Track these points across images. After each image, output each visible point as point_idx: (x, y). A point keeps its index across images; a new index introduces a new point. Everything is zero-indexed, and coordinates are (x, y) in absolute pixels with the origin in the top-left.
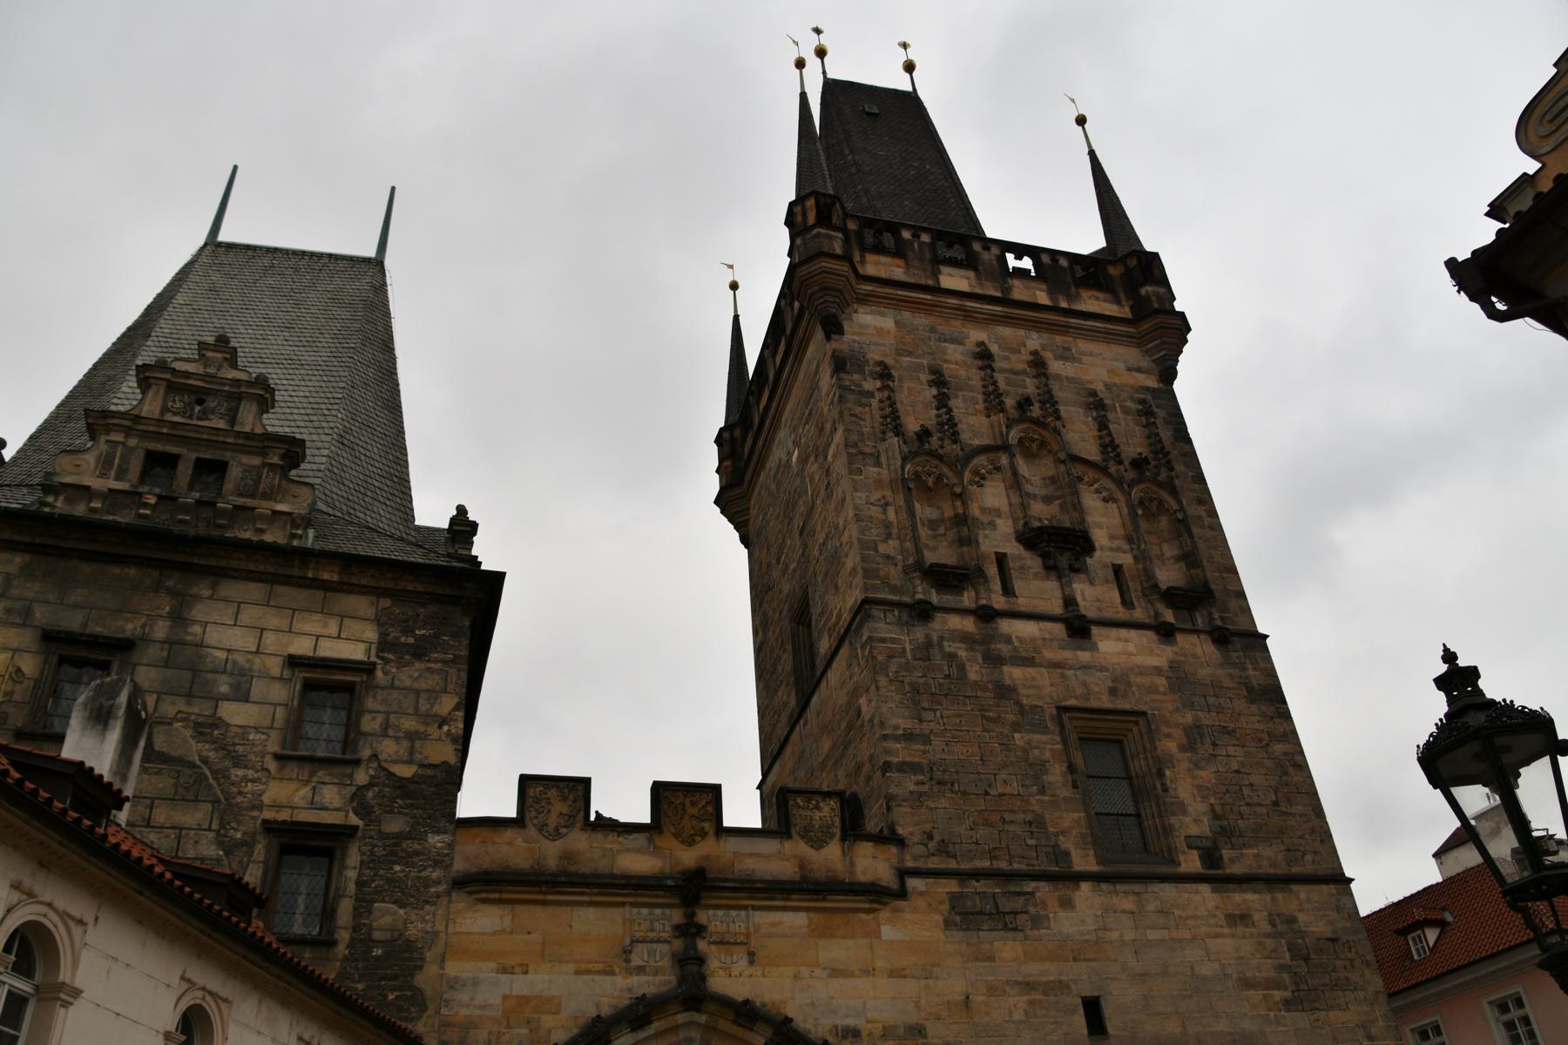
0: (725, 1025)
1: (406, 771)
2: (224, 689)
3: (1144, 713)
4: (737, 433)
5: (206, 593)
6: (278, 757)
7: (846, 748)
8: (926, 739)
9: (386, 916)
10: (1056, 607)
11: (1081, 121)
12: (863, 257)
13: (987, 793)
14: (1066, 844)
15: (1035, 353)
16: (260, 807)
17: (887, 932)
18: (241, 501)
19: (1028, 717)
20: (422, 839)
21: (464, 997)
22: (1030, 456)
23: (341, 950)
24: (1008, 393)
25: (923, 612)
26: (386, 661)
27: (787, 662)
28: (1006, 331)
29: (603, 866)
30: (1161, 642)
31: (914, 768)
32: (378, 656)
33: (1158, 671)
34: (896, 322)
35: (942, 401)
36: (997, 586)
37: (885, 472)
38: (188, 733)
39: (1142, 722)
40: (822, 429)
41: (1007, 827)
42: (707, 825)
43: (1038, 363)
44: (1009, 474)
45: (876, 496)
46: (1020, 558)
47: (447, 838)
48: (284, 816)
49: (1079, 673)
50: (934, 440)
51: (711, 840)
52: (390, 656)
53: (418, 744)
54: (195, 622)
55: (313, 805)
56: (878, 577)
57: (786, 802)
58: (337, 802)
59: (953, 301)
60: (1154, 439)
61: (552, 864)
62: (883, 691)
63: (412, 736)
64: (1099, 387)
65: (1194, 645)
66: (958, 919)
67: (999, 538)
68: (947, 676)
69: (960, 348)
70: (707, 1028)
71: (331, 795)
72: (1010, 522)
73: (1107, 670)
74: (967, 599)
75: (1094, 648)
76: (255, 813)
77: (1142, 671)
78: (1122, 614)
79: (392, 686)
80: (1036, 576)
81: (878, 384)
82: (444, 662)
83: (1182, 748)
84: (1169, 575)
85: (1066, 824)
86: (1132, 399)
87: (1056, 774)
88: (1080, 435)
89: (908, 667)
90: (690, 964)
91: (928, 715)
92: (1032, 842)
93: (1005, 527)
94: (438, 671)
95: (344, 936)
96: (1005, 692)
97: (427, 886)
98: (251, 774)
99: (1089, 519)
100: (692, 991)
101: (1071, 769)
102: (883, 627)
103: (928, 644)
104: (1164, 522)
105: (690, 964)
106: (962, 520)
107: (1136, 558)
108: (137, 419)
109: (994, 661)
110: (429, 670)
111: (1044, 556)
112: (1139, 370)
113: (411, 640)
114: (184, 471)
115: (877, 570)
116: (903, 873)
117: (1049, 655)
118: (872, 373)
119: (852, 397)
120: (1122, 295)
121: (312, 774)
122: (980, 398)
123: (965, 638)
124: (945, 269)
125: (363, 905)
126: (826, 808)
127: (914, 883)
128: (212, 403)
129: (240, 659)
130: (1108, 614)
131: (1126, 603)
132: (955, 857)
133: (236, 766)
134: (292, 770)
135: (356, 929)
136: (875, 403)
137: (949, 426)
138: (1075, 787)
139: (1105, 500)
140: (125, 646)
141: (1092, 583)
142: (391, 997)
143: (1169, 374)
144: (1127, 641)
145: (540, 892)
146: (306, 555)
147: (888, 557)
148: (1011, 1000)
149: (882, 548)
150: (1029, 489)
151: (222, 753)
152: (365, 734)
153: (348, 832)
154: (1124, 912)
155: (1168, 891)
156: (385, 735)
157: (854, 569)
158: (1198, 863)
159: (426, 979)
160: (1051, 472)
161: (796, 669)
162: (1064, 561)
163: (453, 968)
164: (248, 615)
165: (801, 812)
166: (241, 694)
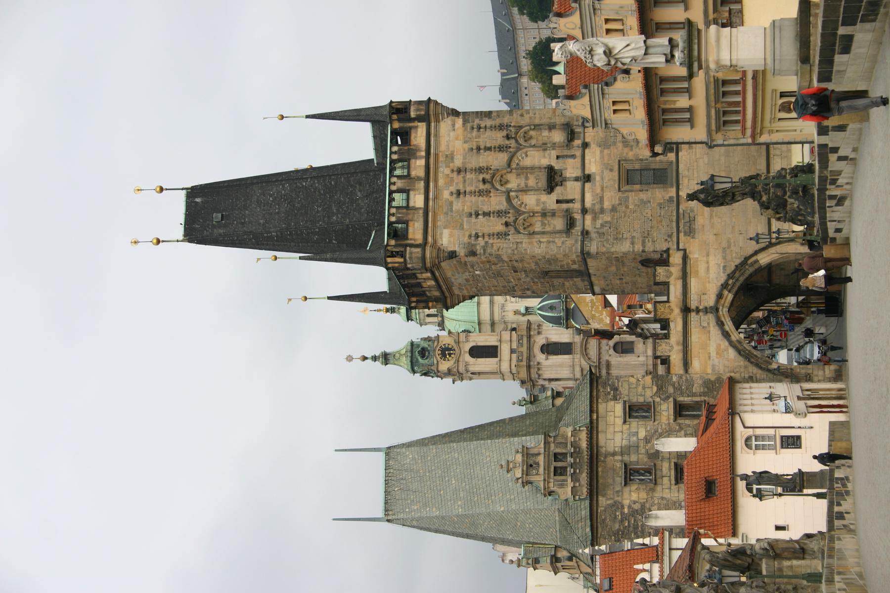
0: (722, 301)
1: (655, 389)
2: (635, 438)
3: (619, 161)
4: (414, 299)
8: (633, 237)
10: (578, 185)
11: (282, 117)
14: (667, 197)
15: (453, 171)
16: (669, 424)
17: (696, 256)
18: (569, 445)
19: (624, 202)
21: (717, 368)
22: (507, 182)
23: (706, 398)
24: (476, 187)
25: (585, 233)
27: (556, 282)
28: (441, 182)
29: (681, 334)
33: (602, 152)
35: (486, 214)
36: (570, 205)
40: (489, 262)
43: (459, 171)
45: (536, 244)
48: (672, 417)
50: (507, 219)
59: (431, 203)
60: (492, 128)
61: (681, 347)
63: (644, 388)
64: (466, 146)
67: (549, 201)
71: (664, 407)
73: (602, 172)
74: (578, 216)
75: (594, 173)
77: (602, 157)
80: (565, 190)
83: (632, 150)
84: (558, 136)
85: (660, 196)
86: (471, 133)
87: (643, 196)
88: (498, 160)
89: (607, 240)
90: (706, 311)
91: (625, 236)
93: (544, 198)
95: (703, 398)
96: (614, 209)
99: (537, 164)
100: (715, 310)
102: (593, 248)
103: (598, 232)
104: (532, 133)
105: (706, 311)
106: (544, 215)
107: (553, 149)
108: (545, 480)
109: (602, 211)
112: (453, 125)
114: (559, 464)
116: (678, 249)
117: (598, 190)
119: (489, 251)
120: (411, 124)
122: (481, 198)
123: (594, 219)
124: (411, 204)
125: (694, 395)
127: (681, 247)
128: (531, 462)
130: (579, 165)
131: (573, 156)
134: (657, 417)
136: (491, 241)
137: (499, 213)
140: (626, 465)
141: (566, 169)
143: (455, 113)
146: (591, 422)
147: (563, 243)
150: (523, 185)
153: (675, 400)
155: (681, 166)
159: (713, 378)
161: (566, 278)
162: (558, 179)
163: (709, 371)
164: (609, 436)
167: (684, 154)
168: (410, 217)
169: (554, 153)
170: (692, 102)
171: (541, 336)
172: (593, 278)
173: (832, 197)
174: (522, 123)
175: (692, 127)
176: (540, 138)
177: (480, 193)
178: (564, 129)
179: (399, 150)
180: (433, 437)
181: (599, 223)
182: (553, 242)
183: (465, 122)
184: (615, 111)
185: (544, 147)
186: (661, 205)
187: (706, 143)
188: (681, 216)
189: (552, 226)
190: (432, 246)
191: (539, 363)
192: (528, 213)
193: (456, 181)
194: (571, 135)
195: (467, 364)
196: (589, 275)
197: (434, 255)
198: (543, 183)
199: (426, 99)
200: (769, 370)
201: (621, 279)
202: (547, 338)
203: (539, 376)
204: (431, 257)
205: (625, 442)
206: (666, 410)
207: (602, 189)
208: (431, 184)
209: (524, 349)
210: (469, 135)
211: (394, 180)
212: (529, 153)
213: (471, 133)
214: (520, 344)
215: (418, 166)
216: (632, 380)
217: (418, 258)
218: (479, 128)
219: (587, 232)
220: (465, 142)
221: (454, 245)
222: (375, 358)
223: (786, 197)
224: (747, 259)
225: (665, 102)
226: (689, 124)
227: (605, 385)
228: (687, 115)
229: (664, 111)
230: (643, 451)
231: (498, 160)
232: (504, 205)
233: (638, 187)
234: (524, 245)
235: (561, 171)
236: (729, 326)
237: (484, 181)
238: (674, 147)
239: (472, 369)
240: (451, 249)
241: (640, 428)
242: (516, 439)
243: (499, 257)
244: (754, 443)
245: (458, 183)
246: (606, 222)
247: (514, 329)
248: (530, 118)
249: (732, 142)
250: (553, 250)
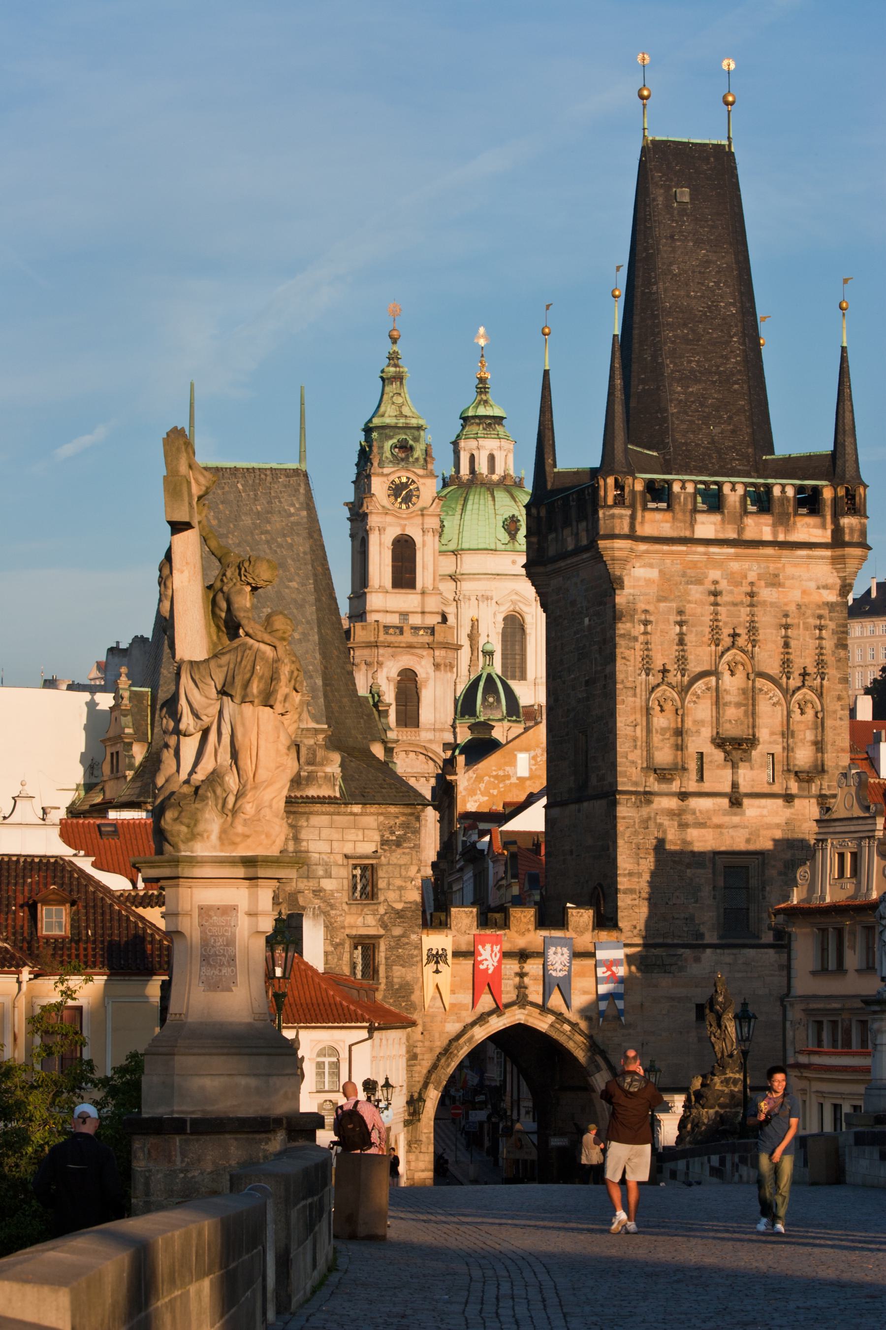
1: (399, 906)
4: (543, 513)
5: (305, 824)
10: (727, 789)
12: (643, 517)
14: (703, 929)
15: (752, 584)
16: (344, 928)
20: (408, 937)
23: (382, 987)
24: (726, 623)
25: (647, 796)
26: (385, 850)
28: (735, 566)
30: (785, 807)
31: (631, 891)
33: (778, 826)
34: (660, 571)
35: (681, 642)
36: (693, 775)
37: (638, 700)
38: (311, 895)
39: (760, 857)
43: (751, 595)
44: (714, 694)
45: (632, 718)
46: (711, 755)
48: (354, 932)
49: (730, 830)
51: (532, 932)
52: (386, 847)
54: (303, 840)
59: (701, 549)
63: (400, 888)
64: (792, 608)
65: (805, 808)
66: (643, 968)
67: (700, 741)
69: (700, 588)
70: (527, 1015)
72: (710, 729)
73: (747, 827)
74: (675, 787)
75: (743, 814)
76: (342, 930)
77: (769, 827)
78: (766, 789)
79: (389, 864)
80: (718, 767)
81: (642, 627)
82: (410, 848)
84: (803, 756)
86: (813, 615)
87: (706, 892)
89: (636, 833)
90: (521, 988)
91: (641, 860)
92: (685, 929)
93: (707, 733)
94: (408, 854)
95: (383, 980)
97: (412, 958)
98: (338, 912)
99: (760, 721)
100: (522, 1001)
101: (714, 887)
103: (649, 818)
104: (810, 713)
105: (521, 988)
106: (679, 732)
109: (683, 826)
110: (404, 853)
111: (725, 752)
112: (826, 587)
113: (394, 838)
117: (716, 820)
118: (641, 621)
121: (362, 910)
123: (671, 813)
124: (700, 517)
125: (389, 967)
129: (323, 856)
133: (332, 909)
134: (354, 908)
135: (387, 978)
136: (638, 646)
137: (682, 660)
138: (714, 898)
139: (774, 705)
141: (751, 769)
142: (403, 1004)
144: (764, 807)
147: (633, 762)
149: (630, 758)
150: (728, 698)
152: (381, 889)
153: (380, 937)
154: (726, 964)
155: (751, 952)
156: (389, 889)
158: (772, 939)
159: (415, 997)
160: (743, 686)
162: (737, 754)
164: (325, 833)
166: (329, 876)
167: (771, 954)
168: (680, 516)
169: (778, 749)
170: (852, 975)
171: (431, 669)
172: (573, 807)
173: (722, 1161)
174: (827, 699)
175: (814, 973)
176: (802, 727)
177: (715, 629)
178: (816, 766)
179: (788, 498)
180: (322, 547)
181: (666, 821)
182: (635, 747)
183: (831, 606)
184: (842, 856)
185: (788, 733)
186: (690, 919)
187: (788, 995)
188: (672, 951)
189: (660, 745)
190: (632, 550)
191: (380, 664)
192: (683, 707)
193: (736, 590)
194: (805, 777)
195: (381, 530)
196: (579, 801)
197: (617, 554)
198: (731, 730)
199: (869, 542)
200: (426, 1085)
201: (571, 852)
202: (427, 680)
204: (613, 549)
205: (315, 857)
206: (365, 922)
207: (719, 826)
208: (732, 550)
209: (408, 637)
210: (809, 612)
211: (740, 490)
212: (778, 708)
213: (813, 615)
214: (415, 629)
215: (760, 527)
216: (413, 870)
217: (613, 528)
218: (821, 628)
219: (649, 802)
220: (799, 606)
221: (634, 587)
222: (393, 358)
223: (717, 1108)
225: (853, 933)
226: (819, 968)
227: (406, 826)
228: (832, 965)
229: (840, 932)
230: (302, 885)
231: (768, 658)
232: (695, 668)
233: (721, 883)
234: (631, 699)
235: (749, 760)
236: (497, 1024)
237: (734, 635)
238: (782, 942)
239: (374, 540)
240: (626, 583)
241: (336, 883)
242: (319, 682)
243: (611, 658)
244: (327, 1060)
245: (731, 594)
247: (444, 619)
248: (835, 712)
249: (790, 1034)
250: (622, 747)
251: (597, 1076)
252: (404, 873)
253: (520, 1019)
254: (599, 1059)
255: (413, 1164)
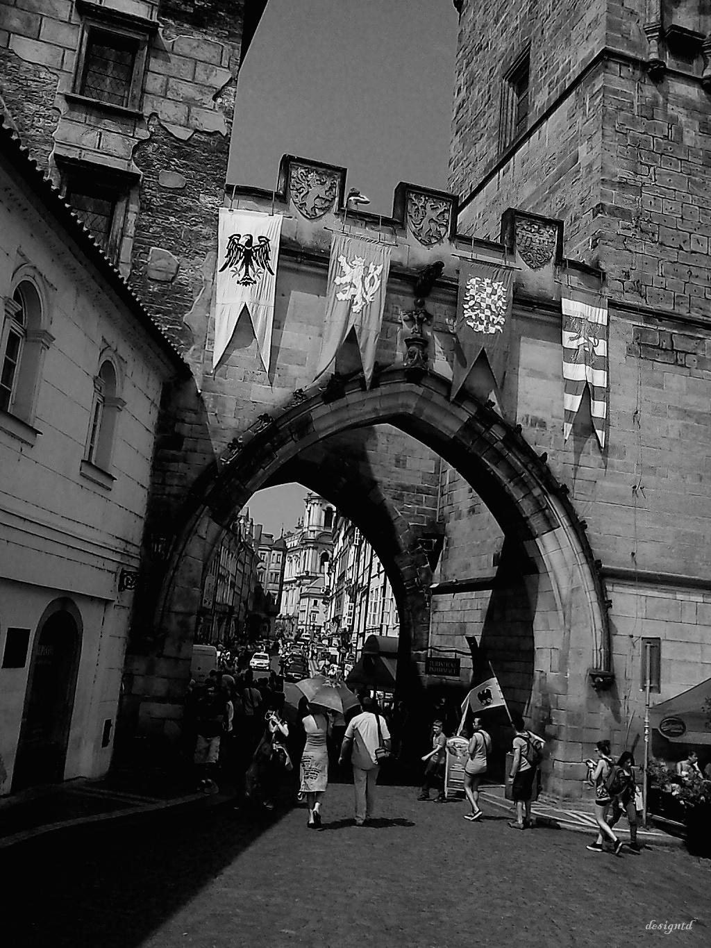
0: (438, 399)
1: (183, 134)
6: (68, 99)
7: (553, 192)
9: (160, 260)
13: (681, 248)
26: (167, 26)
31: (624, 214)
32: (158, 19)
41: (692, 280)
42: (443, 230)
47: (217, 200)
48: (73, 154)
53: (194, 109)
55: (98, 150)
56: (619, 31)
57: (513, 223)
58: (121, 151)
62: (607, 140)
63: (189, 102)
66: (637, 348)
68: (666, 137)
70: (423, 398)
76: (47, 148)
89: (633, 121)
97: (197, 239)
103: (655, 104)
115: (620, 24)
123: (688, 105)
125: (141, 247)
126: (546, 235)
132: (644, 297)
145: (296, 262)
147: (632, 12)
148: (670, 422)
151: (14, 86)
156: (165, 97)
157: (596, 21)
165: (523, 232)
203: (314, 504)
224: (561, 493)
246: (680, 132)
251: (547, 537)
252: (201, 76)
253: (408, 406)
254: (552, 501)
255: (139, 681)
